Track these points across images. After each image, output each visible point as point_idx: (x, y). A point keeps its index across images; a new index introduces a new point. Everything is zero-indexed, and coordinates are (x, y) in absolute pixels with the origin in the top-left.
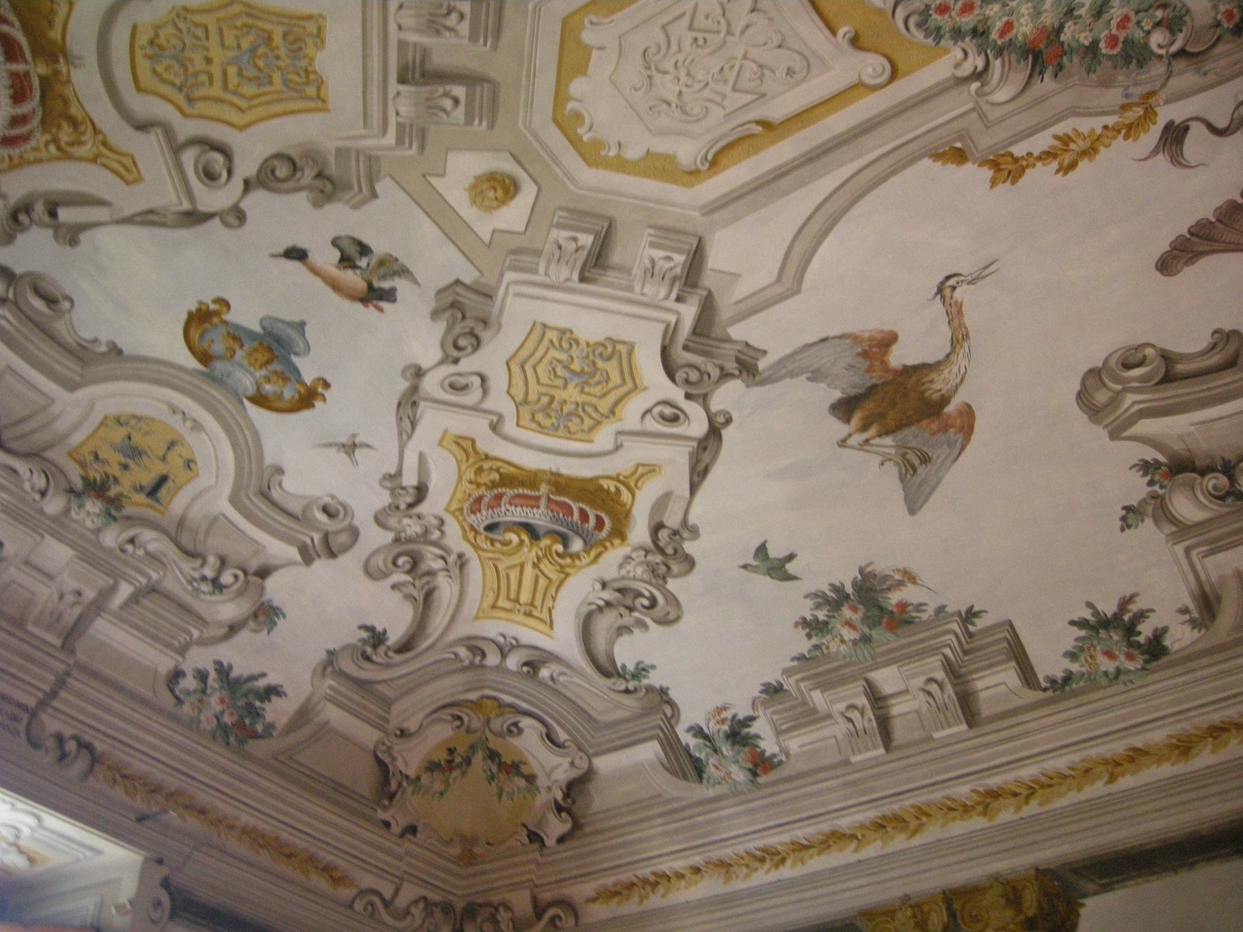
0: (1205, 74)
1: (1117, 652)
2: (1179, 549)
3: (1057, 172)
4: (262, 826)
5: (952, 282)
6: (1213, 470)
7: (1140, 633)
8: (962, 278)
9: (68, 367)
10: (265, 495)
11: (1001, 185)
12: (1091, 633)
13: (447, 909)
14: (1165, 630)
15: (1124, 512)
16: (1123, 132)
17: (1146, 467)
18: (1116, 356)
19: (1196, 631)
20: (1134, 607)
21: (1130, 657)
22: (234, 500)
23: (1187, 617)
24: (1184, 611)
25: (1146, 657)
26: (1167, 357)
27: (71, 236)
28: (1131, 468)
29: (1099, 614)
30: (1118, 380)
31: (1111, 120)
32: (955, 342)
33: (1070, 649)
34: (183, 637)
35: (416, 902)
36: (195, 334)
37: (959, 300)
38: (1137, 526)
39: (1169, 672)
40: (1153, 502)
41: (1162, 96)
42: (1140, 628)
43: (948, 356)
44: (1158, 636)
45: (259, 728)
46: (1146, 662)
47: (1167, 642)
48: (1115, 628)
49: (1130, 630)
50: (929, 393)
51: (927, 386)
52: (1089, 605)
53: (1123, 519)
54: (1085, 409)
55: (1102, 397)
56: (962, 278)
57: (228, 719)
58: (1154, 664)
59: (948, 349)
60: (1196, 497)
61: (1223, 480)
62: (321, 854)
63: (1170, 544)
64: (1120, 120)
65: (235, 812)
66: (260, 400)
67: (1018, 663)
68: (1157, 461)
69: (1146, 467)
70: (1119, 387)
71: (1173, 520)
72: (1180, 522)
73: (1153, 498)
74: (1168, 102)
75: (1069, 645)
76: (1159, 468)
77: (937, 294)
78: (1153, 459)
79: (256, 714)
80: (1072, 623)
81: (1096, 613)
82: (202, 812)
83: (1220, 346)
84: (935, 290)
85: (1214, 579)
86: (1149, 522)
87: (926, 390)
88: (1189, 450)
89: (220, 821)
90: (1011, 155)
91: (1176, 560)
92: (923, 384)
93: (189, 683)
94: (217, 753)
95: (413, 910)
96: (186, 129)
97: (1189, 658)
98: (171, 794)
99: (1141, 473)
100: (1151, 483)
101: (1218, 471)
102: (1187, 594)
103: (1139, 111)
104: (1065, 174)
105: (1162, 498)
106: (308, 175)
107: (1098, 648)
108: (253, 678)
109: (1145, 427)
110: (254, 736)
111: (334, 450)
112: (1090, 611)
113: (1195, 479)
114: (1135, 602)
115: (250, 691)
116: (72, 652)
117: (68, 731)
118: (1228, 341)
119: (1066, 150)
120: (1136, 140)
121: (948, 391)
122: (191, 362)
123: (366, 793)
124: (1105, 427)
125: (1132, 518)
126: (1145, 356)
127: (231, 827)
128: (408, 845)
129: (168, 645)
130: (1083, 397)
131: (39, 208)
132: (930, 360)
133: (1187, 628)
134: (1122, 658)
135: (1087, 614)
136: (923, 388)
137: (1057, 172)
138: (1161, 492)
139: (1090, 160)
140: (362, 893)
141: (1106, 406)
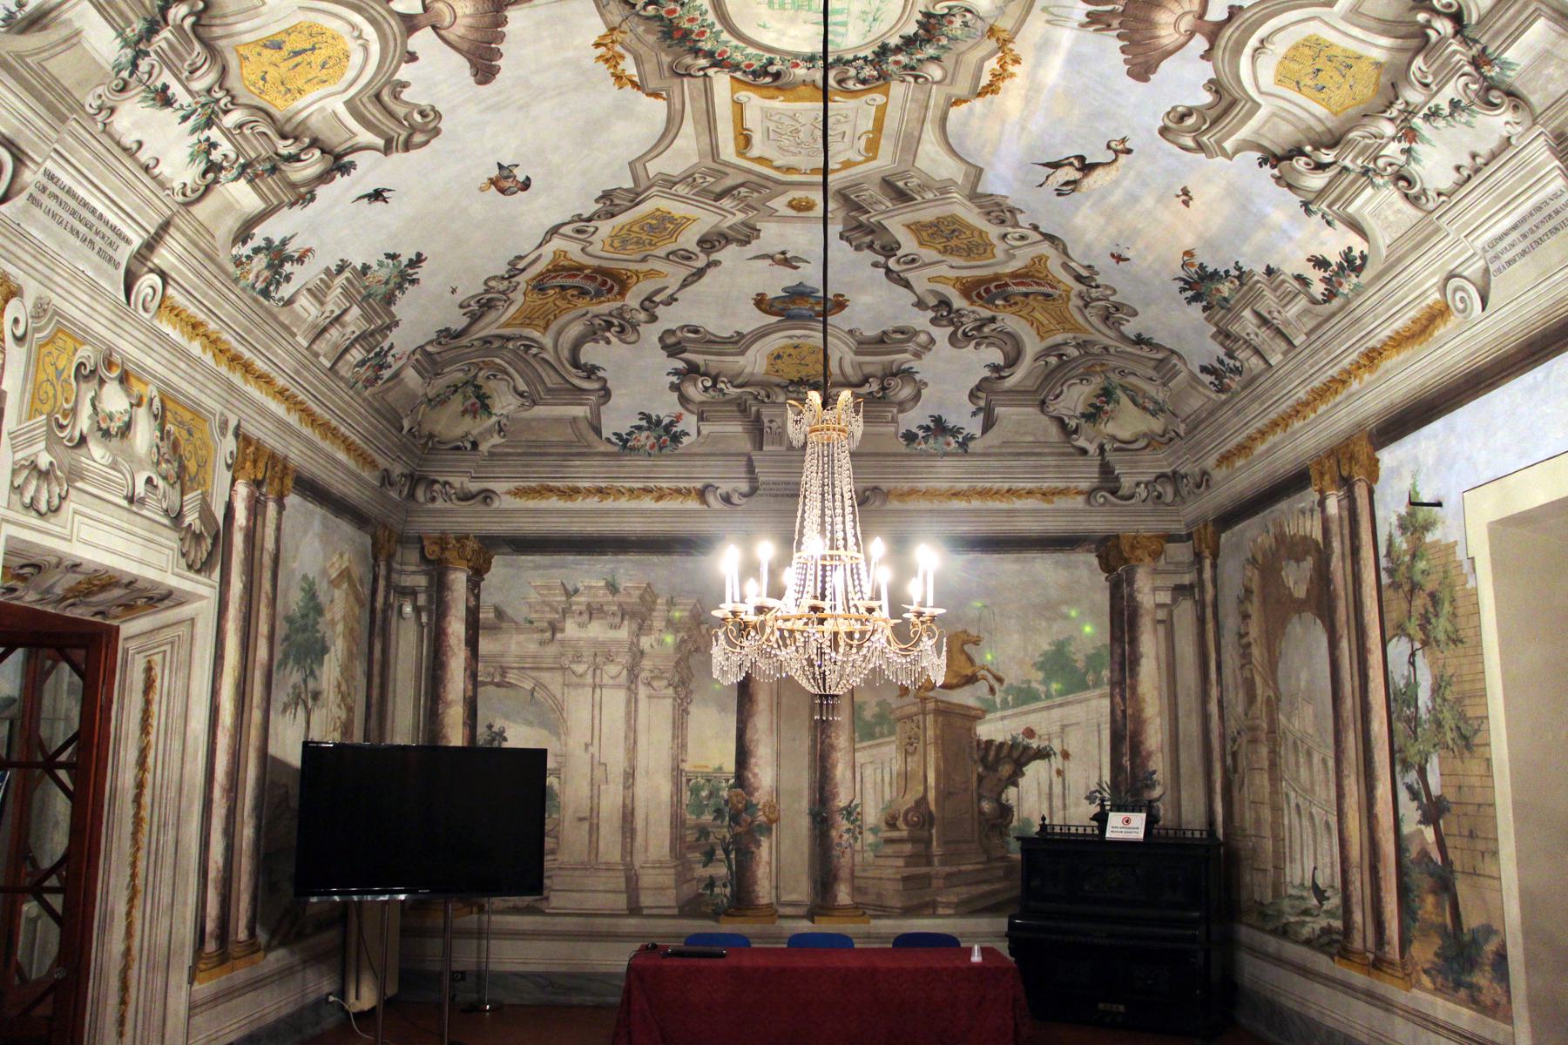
23: (14, 9)
85: (66, 16)
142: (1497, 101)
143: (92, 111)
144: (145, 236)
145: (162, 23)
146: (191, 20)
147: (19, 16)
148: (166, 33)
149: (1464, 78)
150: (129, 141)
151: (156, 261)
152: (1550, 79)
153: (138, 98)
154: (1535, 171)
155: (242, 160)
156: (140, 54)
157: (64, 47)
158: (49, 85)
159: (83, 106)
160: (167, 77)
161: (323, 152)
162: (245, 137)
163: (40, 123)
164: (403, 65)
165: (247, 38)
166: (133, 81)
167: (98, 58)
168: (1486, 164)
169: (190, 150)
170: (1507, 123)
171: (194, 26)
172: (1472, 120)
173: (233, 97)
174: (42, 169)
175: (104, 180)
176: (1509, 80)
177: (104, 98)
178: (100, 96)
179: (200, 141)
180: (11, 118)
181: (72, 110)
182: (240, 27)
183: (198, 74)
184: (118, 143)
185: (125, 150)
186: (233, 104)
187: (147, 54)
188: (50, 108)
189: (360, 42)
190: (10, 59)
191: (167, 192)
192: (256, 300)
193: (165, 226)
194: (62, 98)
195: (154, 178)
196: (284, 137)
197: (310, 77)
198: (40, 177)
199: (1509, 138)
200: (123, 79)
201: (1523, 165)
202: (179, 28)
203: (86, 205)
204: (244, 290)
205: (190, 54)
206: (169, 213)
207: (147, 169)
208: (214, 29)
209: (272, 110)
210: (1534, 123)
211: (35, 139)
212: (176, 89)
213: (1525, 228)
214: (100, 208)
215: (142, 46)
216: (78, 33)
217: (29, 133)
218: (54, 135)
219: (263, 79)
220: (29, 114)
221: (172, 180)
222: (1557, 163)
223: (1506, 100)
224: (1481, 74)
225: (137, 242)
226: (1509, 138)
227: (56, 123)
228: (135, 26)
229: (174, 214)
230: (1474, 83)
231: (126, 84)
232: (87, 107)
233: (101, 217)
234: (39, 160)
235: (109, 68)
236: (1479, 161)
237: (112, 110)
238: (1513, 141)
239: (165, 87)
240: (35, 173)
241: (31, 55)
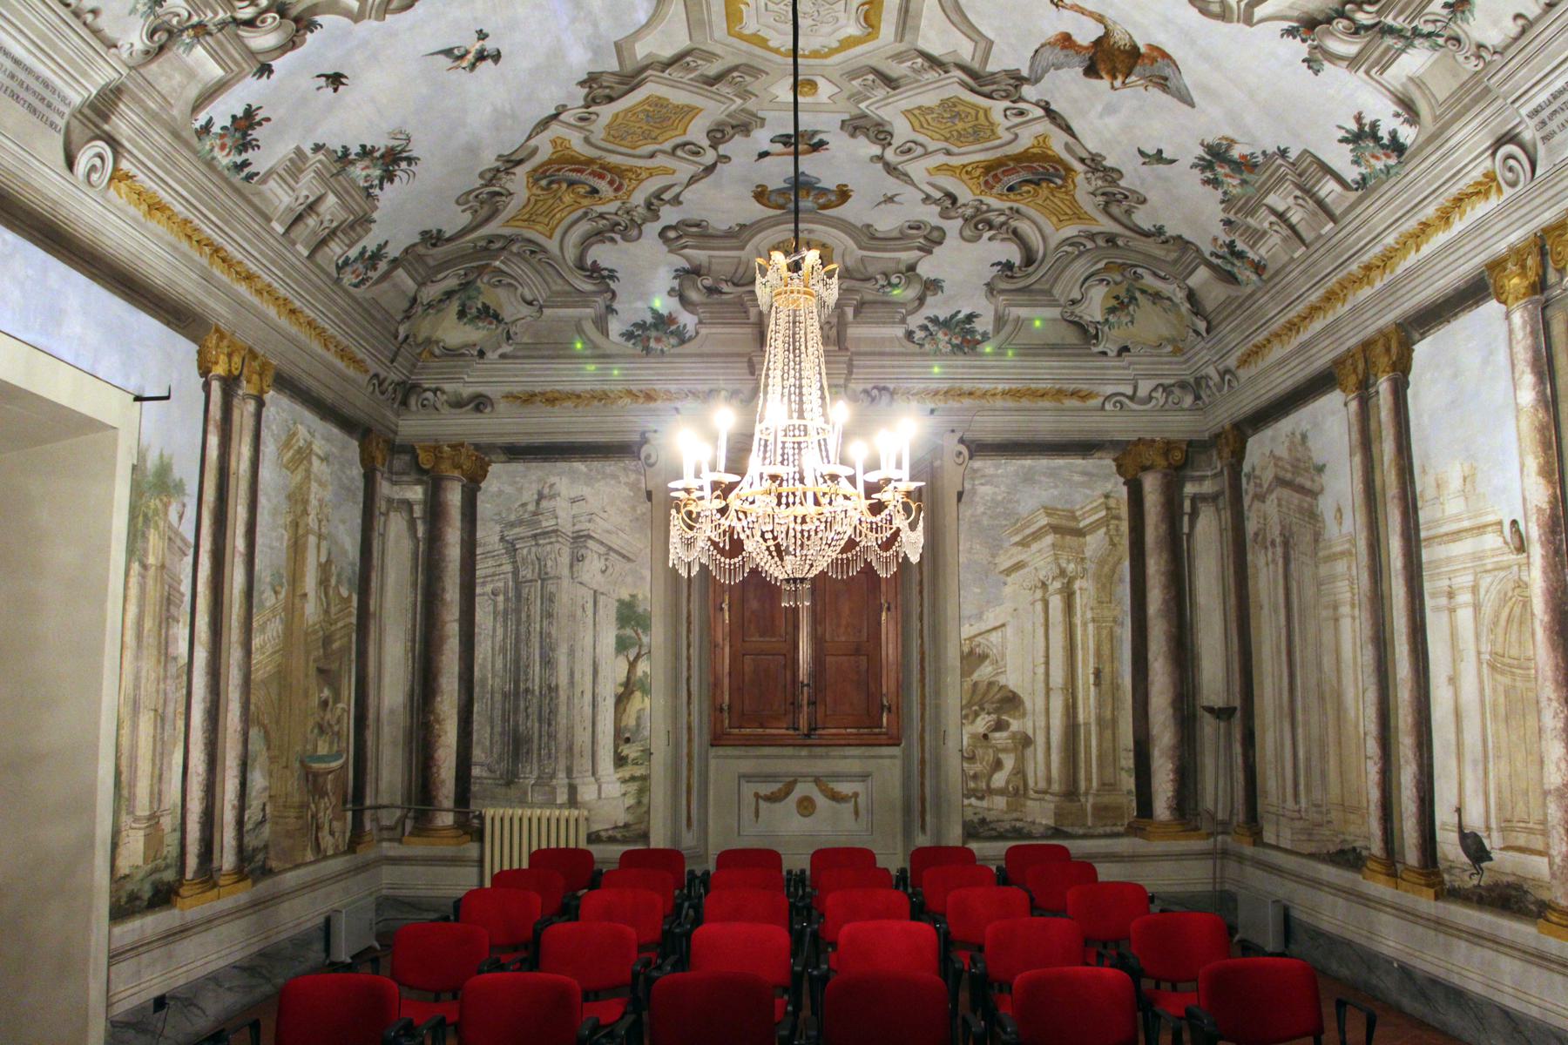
4: (1014, 386)
6: (1334, 18)
9: (734, 242)
10: (873, 238)
13: (1183, 385)
17: (1291, 32)
22: (861, 248)
23: (1402, 119)
27: (676, 201)
34: (898, 317)
35: (1155, 389)
36: (765, 201)
44: (1394, 135)
45: (979, 337)
49: (1377, 139)
53: (1309, 67)
57: (955, 341)
61: (1345, 22)
62: (1065, 387)
65: (993, 386)
66: (824, 207)
71: (1342, 58)
79: (972, 331)
81: (1347, 131)
82: (971, 394)
89: (985, 394)
93: (919, 335)
94: (961, 360)
95: (1154, 394)
96: (668, 146)
97: (1420, 149)
98: (946, 393)
106: (729, 130)
108: (953, 317)
110: (979, 342)
111: (883, 205)
115: (958, 323)
116: (847, 349)
117: (869, 386)
122: (779, 212)
123: (1076, 342)
127: (994, 395)
128: (1127, 358)
129: (894, 323)
131: (654, 201)
133: (1406, 126)
134: (1383, 158)
135: (1342, 134)
140: (1108, 398)
142: (156, 38)
143: (1481, 65)
146: (1367, 8)
148: (1389, 20)
149: (186, 14)
150: (1513, 29)
152: (170, 78)
154: (85, 74)
156: (1416, 33)
159: (1476, 73)
163: (1488, 112)
166: (1446, 33)
167: (1429, 63)
168: (85, 24)
170: (132, 45)
172: (139, 14)
174: (1527, 119)
176: (175, 48)
178: (1466, 58)
184: (1516, 39)
185: (1523, 31)
187: (1415, 29)
188: (1475, 101)
198: (1532, 123)
199: (116, 46)
200: (1446, 41)
201: (89, 62)
210: (130, 68)
213: (22, 75)
215: (1409, 34)
216: (1411, 79)
218: (1500, 101)
222: (94, 92)
223: (157, 45)
224: (187, 29)
226: (116, 46)
227: (1489, 98)
230: (179, 22)
231: (1450, 38)
234: (1518, 120)
235: (1437, 55)
236: (89, 18)
237: (1480, 46)
238: (113, 50)
240: (1527, 127)
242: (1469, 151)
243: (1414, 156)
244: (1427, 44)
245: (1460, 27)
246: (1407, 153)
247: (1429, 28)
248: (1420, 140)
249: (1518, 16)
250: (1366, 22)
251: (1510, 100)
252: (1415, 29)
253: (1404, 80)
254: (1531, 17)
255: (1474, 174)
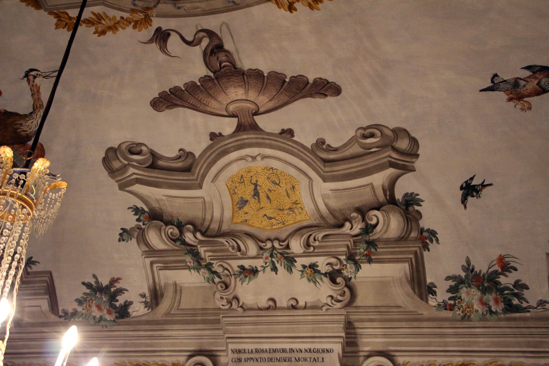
0: (179, 8)
1: (103, 308)
2: (148, 261)
3: (95, 33)
5: (33, 73)
6: (172, 224)
7: (117, 301)
8: (39, 73)
11: (61, 29)
12: (92, 292)
14: (131, 303)
15: (121, 231)
16: (133, 24)
17: (137, 210)
18: (127, 144)
19: (146, 309)
20: (118, 285)
21: (109, 312)
23: (144, 300)
24: (143, 296)
25: (117, 315)
26: (154, 155)
28: (129, 208)
29: (99, 284)
30: (126, 159)
31: (126, 15)
32: (35, 107)
33: (80, 298)
37: (38, 85)
38: (127, 241)
39: (126, 327)
40: (138, 231)
41: (154, 12)
42: (118, 298)
43: (31, 113)
44: (127, 305)
46: (117, 318)
47: (130, 310)
48: (106, 294)
49: (113, 297)
50: (20, 130)
51: (18, 126)
52: (94, 276)
53: (121, 235)
54: (107, 168)
55: (116, 165)
56: (39, 73)
58: (121, 320)
59: (31, 110)
60: (161, 235)
61: (176, 231)
63: (143, 257)
64: (130, 16)
67: (50, 297)
68: (143, 209)
69: (137, 210)
70: (126, 162)
71: (147, 244)
72: (151, 247)
73: (138, 228)
74: (158, 16)
75: (79, 295)
76: (144, 214)
77: (25, 77)
78: (141, 207)
80: (84, 283)
81: (97, 282)
83: (183, 158)
84: (24, 74)
85: (162, 284)
86: (134, 241)
87: (18, 129)
88: (161, 209)
90: (67, 14)
91: (145, 267)
92: (17, 124)
97: (139, 323)
99: (134, 213)
100: (138, 220)
101: (175, 226)
102: (147, 286)
103: (141, 16)
104: (99, 36)
105: (144, 230)
107: (94, 302)
109: (138, 188)
112: (94, 280)
113: (164, 226)
114: (119, 283)
118: (186, 158)
119: (100, 23)
120: (140, 31)
121: (31, 133)
124: (117, 181)
125: (125, 236)
126: (141, 151)
130: (106, 161)
132: (21, 112)
133: (143, 306)
134: (105, 311)
135: (93, 281)
136: (16, 127)
137: (95, 33)
138: (143, 227)
139: (114, 33)
141: (118, 170)
143: (227, 307)
144: (342, 340)
145: (194, 248)
146: (198, 235)
147: (149, 300)
148: (202, 250)
150: (263, 302)
151: (367, 349)
153: (239, 283)
155: (343, 258)
156: (209, 267)
157: (178, 294)
158: (192, 314)
159: (220, 309)
160: (235, 264)
161: (378, 209)
162: (319, 247)
164: (294, 138)
165: (228, 214)
166: (224, 279)
167: (196, 285)
169: (305, 279)
171: (203, 234)
173: (277, 239)
174: (230, 351)
175: (274, 332)
177: (224, 297)
178: (222, 298)
179: (302, 271)
180: (190, 341)
181: (218, 314)
182: (217, 214)
183: (242, 247)
184: (260, 309)
185: (268, 308)
186: (283, 241)
187: (211, 264)
188: (204, 322)
189: (259, 158)
190: (165, 318)
191: (324, 308)
192: (508, 319)
193: (349, 326)
194: (206, 314)
195: (305, 308)
196: (341, 226)
197: (285, 194)
198: (231, 355)
200: (219, 282)
202: (201, 242)
203: (275, 351)
204: (481, 320)
205: (225, 245)
206: (343, 317)
207: (294, 307)
208: (212, 226)
209: (305, 224)
211: (212, 341)
212: (247, 263)
214: (287, 346)
215: (203, 264)
216: (175, 284)
217: (206, 341)
218: (221, 332)
219: (270, 218)
220: (199, 332)
221: (319, 300)
225: (338, 348)
227: (216, 326)
228: (187, 260)
229: (347, 316)
231: (224, 283)
232: (222, 307)
233: (292, 350)
234: (224, 348)
235: (207, 284)
237: (236, 298)
239: (242, 267)
240: (227, 356)
241: (171, 310)
242: (173, 345)
243: (129, 324)
244: (207, 275)
245: (236, 281)
246: (126, 320)
247: (219, 270)
248: (144, 318)
249: (273, 300)
250: (187, 240)
251: (226, 335)
252: (211, 264)
253: (171, 282)
254: (278, 305)
255: (166, 359)
